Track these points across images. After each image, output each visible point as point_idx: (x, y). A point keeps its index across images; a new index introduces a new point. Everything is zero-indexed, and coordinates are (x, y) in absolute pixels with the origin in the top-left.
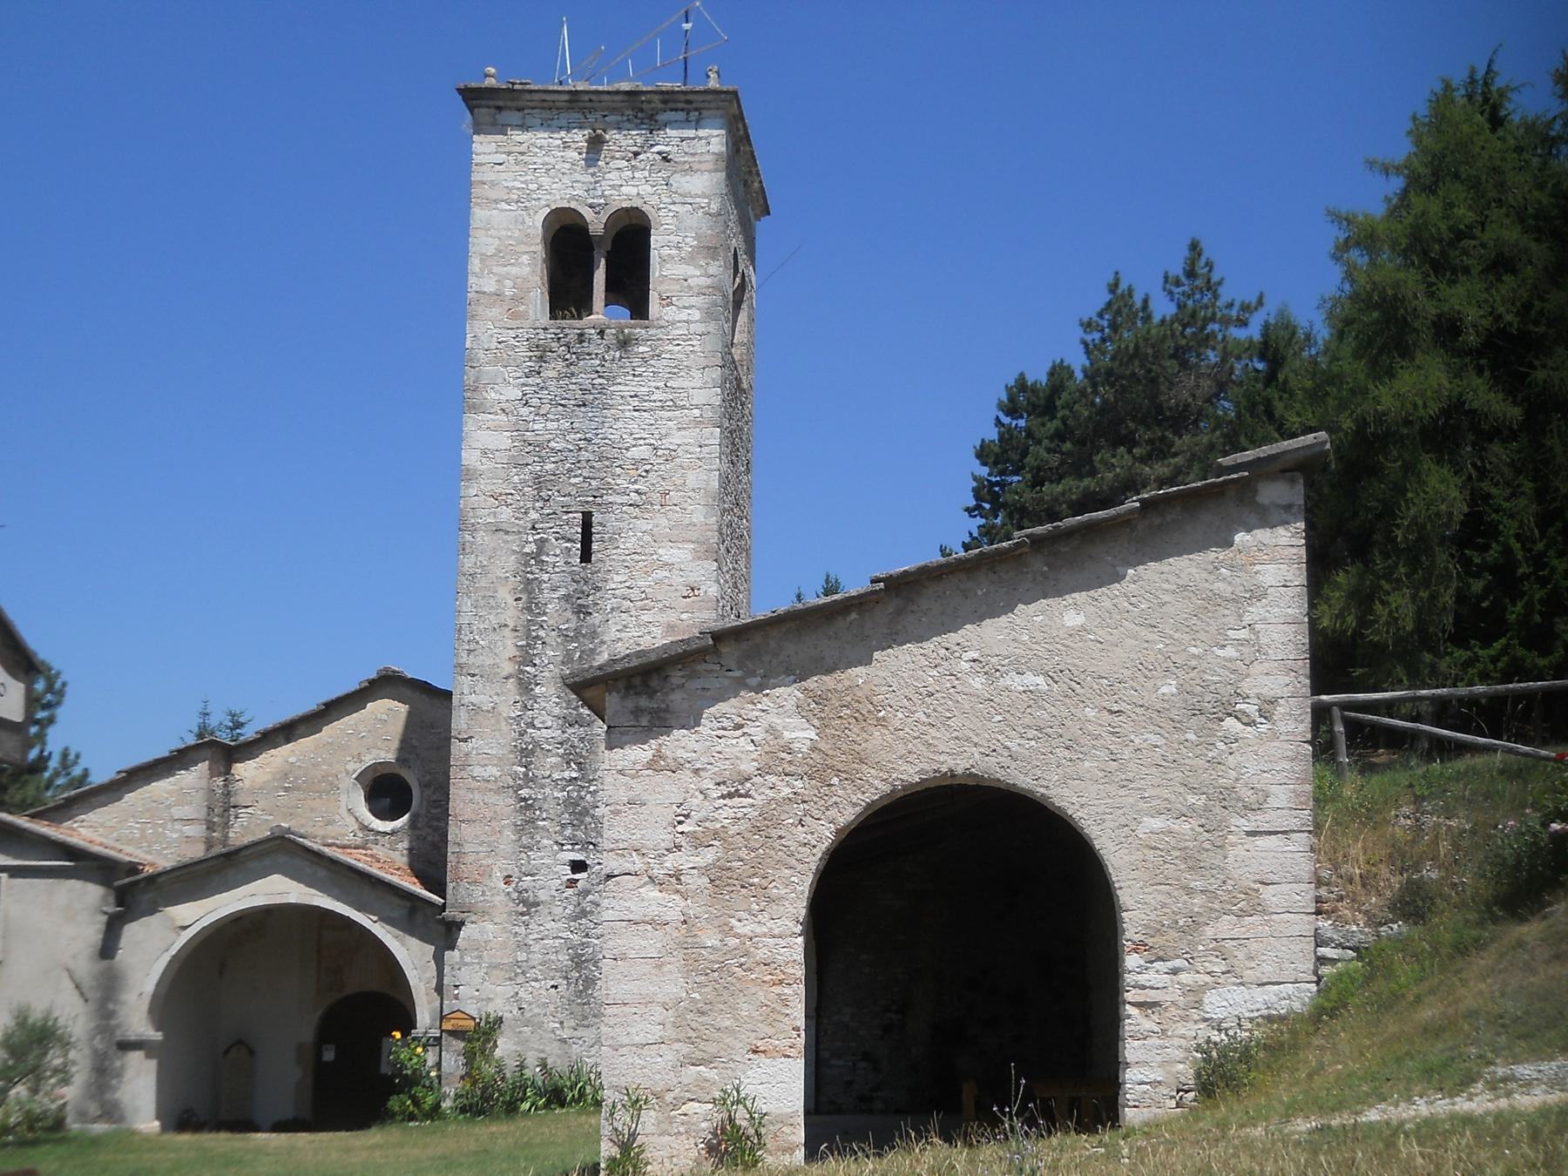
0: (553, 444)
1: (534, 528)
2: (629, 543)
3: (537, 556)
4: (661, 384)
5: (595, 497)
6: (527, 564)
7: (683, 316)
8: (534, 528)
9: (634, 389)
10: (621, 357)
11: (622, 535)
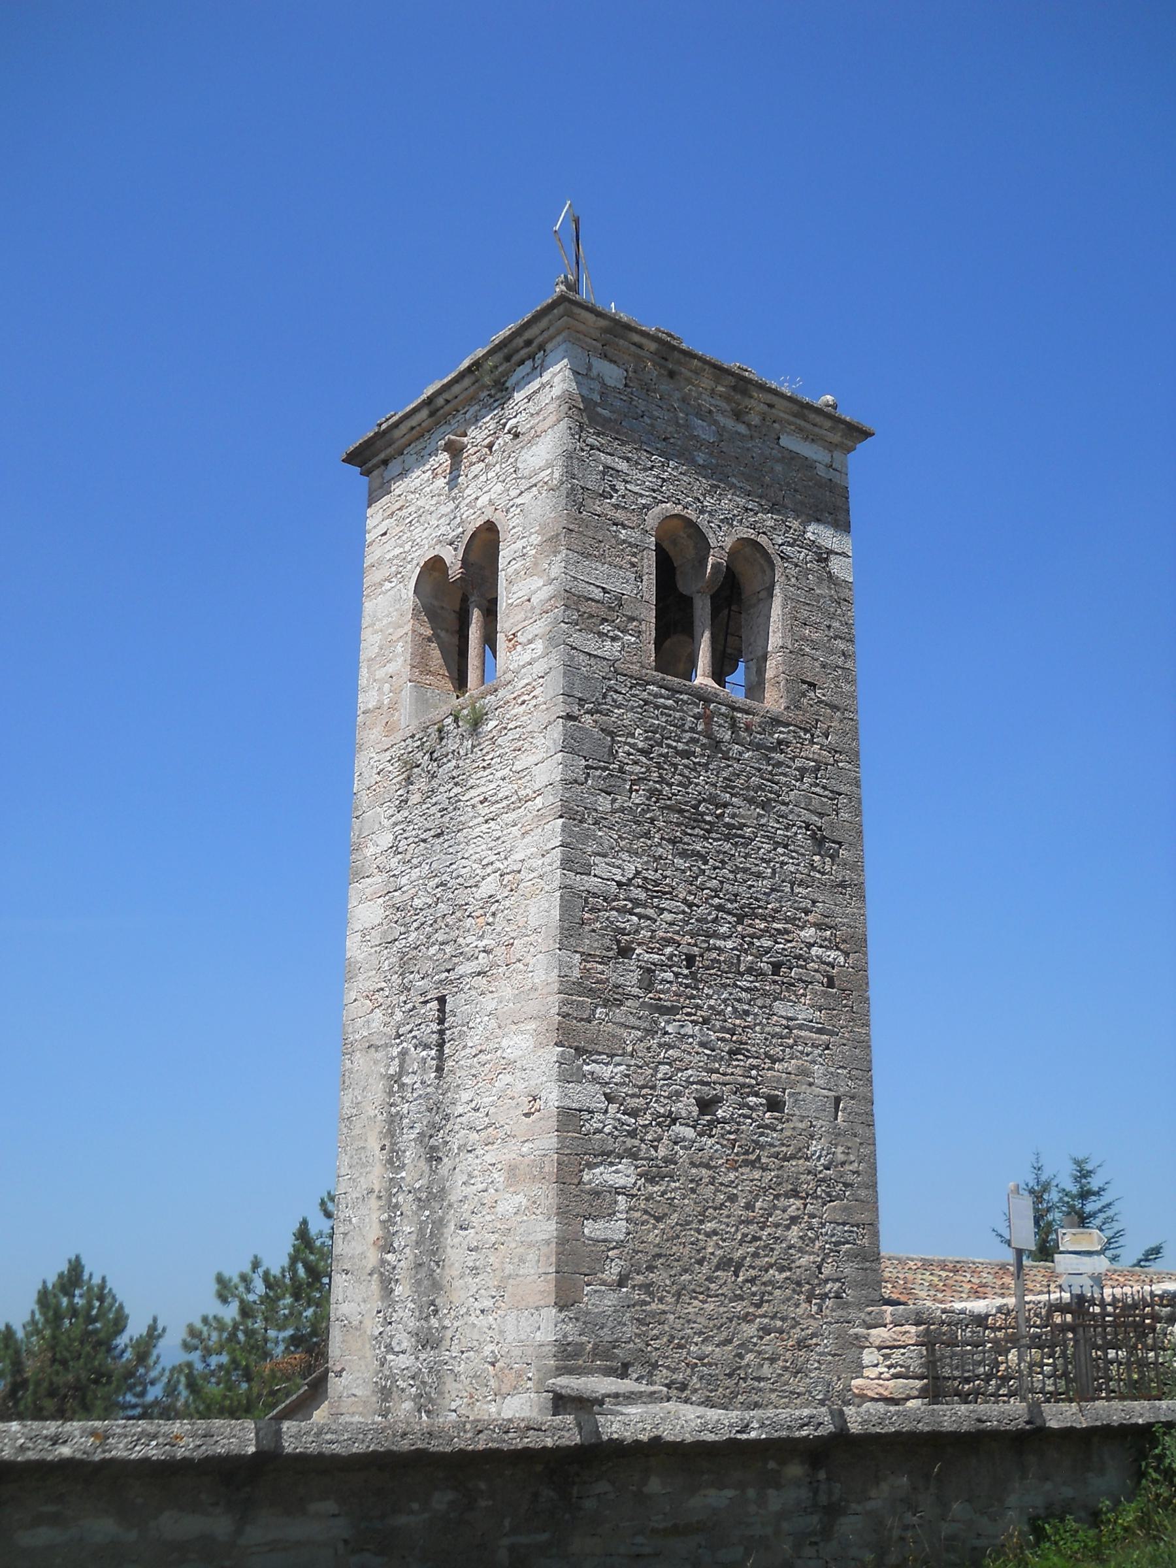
0: (417, 902)
1: (399, 1036)
2: (474, 1040)
3: (396, 1079)
4: (506, 772)
5: (448, 971)
6: (391, 1093)
7: (527, 657)
8: (399, 1036)
9: (484, 789)
10: (473, 746)
11: (471, 1025)
